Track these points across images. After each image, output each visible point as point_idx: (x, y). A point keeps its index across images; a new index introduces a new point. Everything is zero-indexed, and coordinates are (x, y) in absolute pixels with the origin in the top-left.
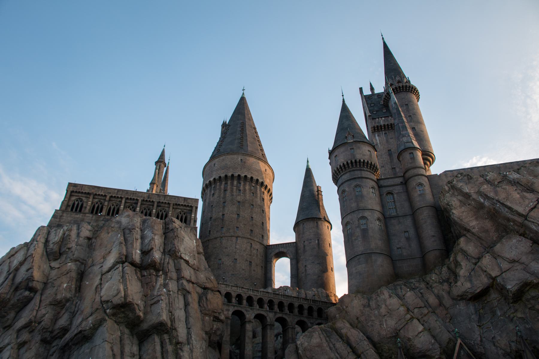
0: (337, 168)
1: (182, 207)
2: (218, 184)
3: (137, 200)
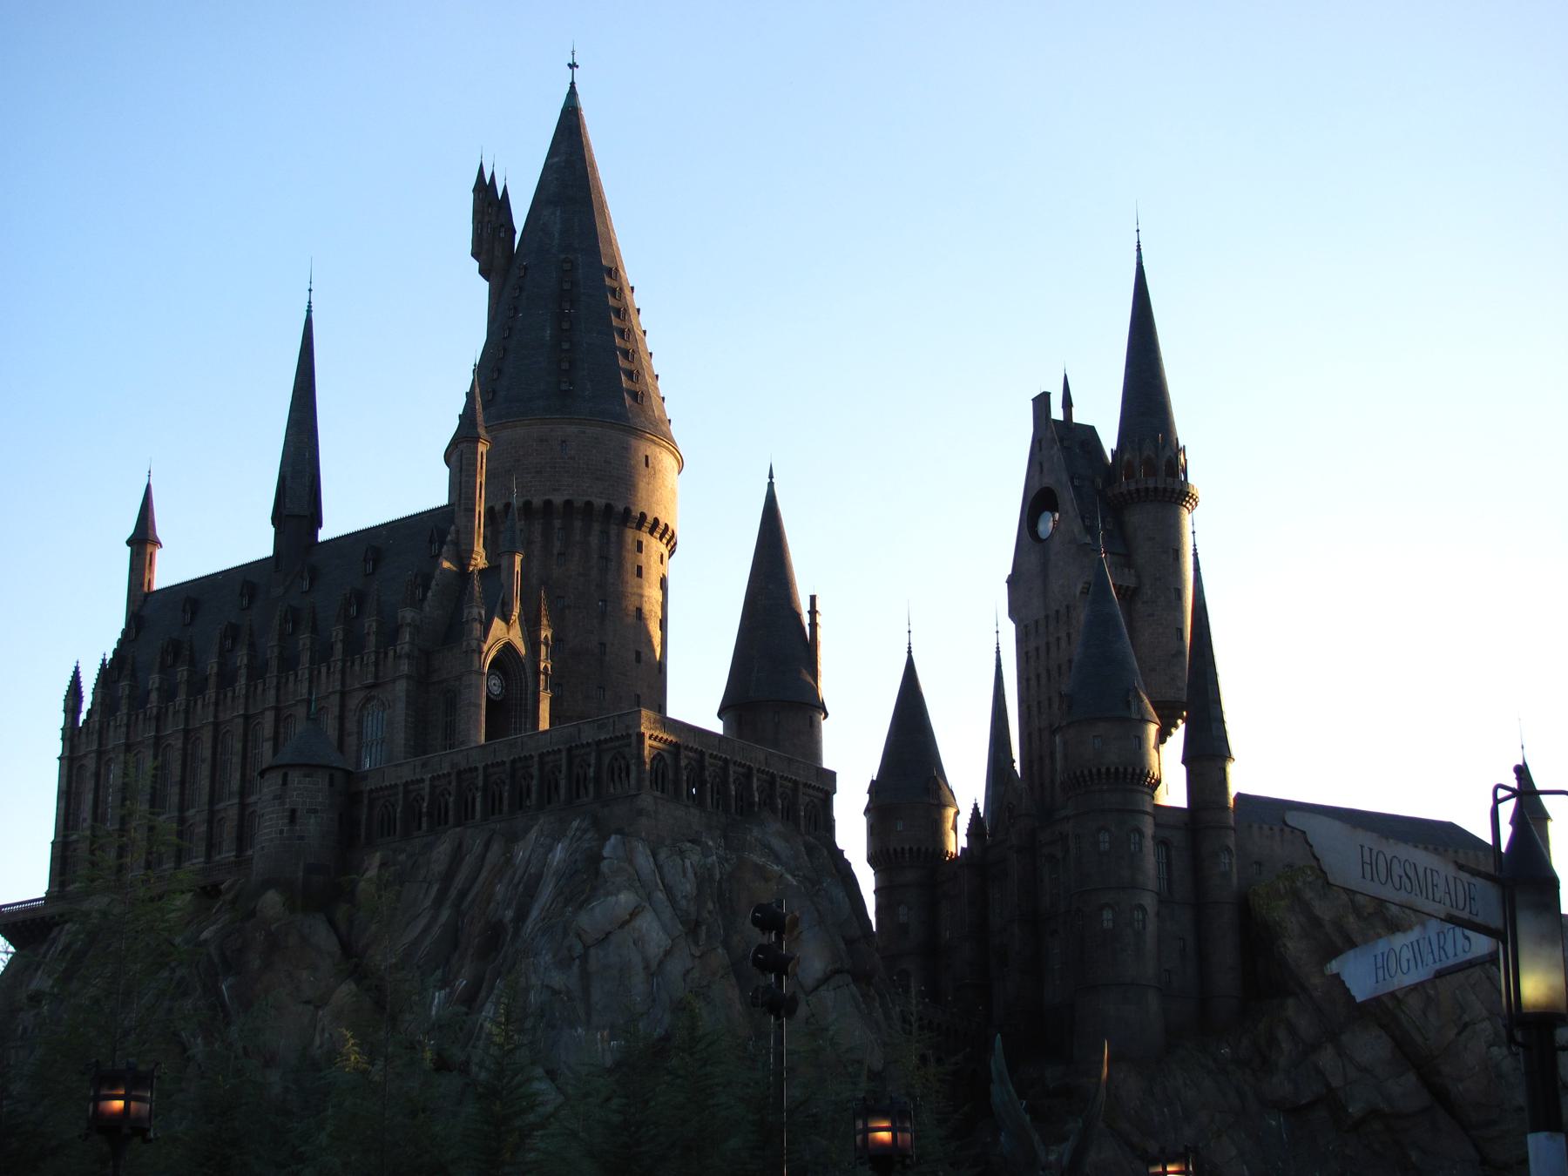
0: (1099, 770)
1: (811, 791)
2: (578, 524)
3: (750, 768)
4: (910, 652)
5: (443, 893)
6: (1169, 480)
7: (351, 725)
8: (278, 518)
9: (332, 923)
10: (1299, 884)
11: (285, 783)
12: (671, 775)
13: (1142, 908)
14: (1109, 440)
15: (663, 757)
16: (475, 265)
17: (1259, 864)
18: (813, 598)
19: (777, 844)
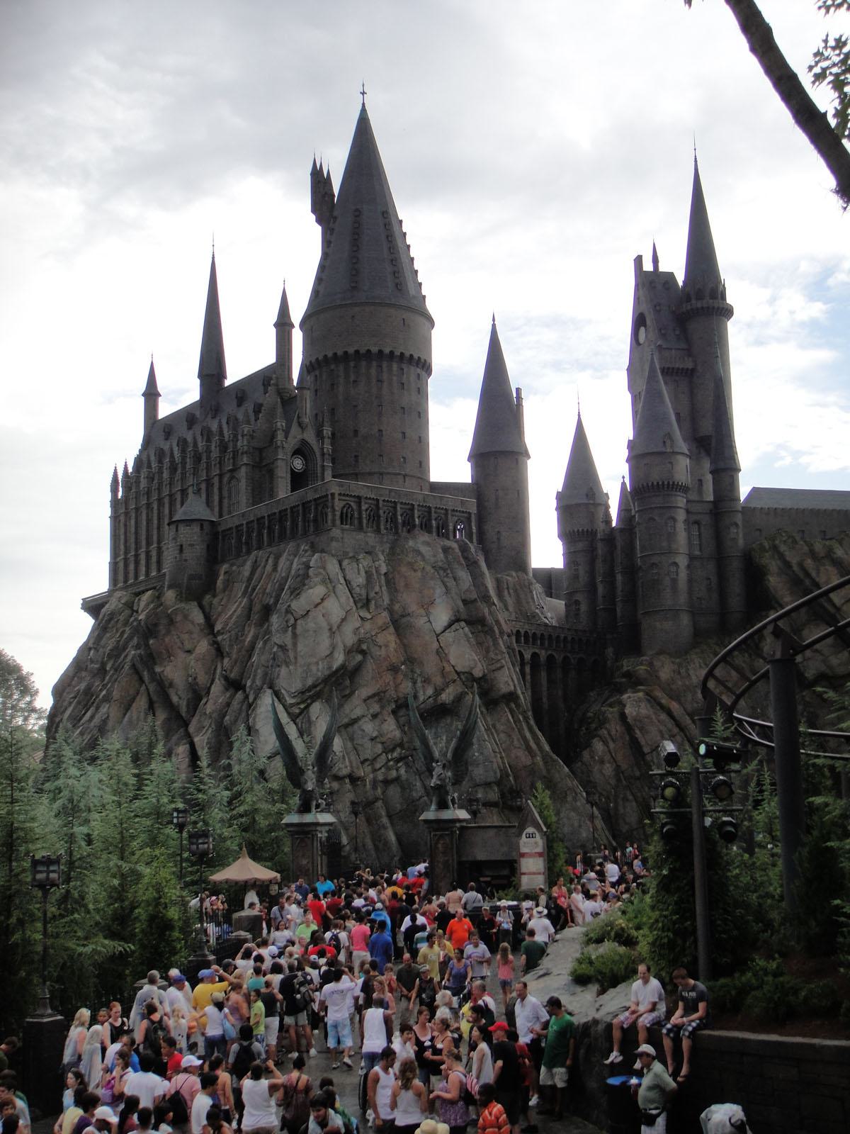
1: (457, 514)
3: (413, 505)
4: (579, 415)
5: (247, 587)
6: (711, 301)
7: (225, 494)
8: (202, 375)
9: (201, 607)
10: (777, 542)
11: (177, 531)
12: (356, 515)
13: (676, 564)
14: (680, 278)
15: (350, 505)
16: (313, 217)
17: (760, 530)
18: (518, 390)
19: (424, 549)
